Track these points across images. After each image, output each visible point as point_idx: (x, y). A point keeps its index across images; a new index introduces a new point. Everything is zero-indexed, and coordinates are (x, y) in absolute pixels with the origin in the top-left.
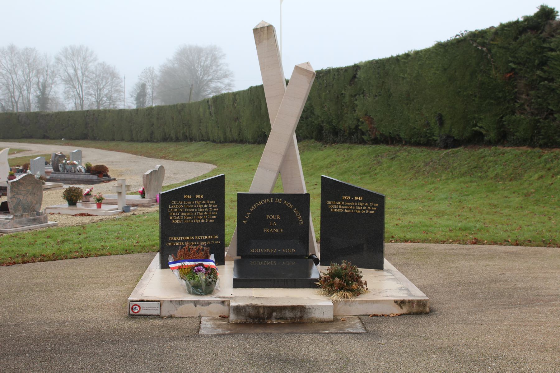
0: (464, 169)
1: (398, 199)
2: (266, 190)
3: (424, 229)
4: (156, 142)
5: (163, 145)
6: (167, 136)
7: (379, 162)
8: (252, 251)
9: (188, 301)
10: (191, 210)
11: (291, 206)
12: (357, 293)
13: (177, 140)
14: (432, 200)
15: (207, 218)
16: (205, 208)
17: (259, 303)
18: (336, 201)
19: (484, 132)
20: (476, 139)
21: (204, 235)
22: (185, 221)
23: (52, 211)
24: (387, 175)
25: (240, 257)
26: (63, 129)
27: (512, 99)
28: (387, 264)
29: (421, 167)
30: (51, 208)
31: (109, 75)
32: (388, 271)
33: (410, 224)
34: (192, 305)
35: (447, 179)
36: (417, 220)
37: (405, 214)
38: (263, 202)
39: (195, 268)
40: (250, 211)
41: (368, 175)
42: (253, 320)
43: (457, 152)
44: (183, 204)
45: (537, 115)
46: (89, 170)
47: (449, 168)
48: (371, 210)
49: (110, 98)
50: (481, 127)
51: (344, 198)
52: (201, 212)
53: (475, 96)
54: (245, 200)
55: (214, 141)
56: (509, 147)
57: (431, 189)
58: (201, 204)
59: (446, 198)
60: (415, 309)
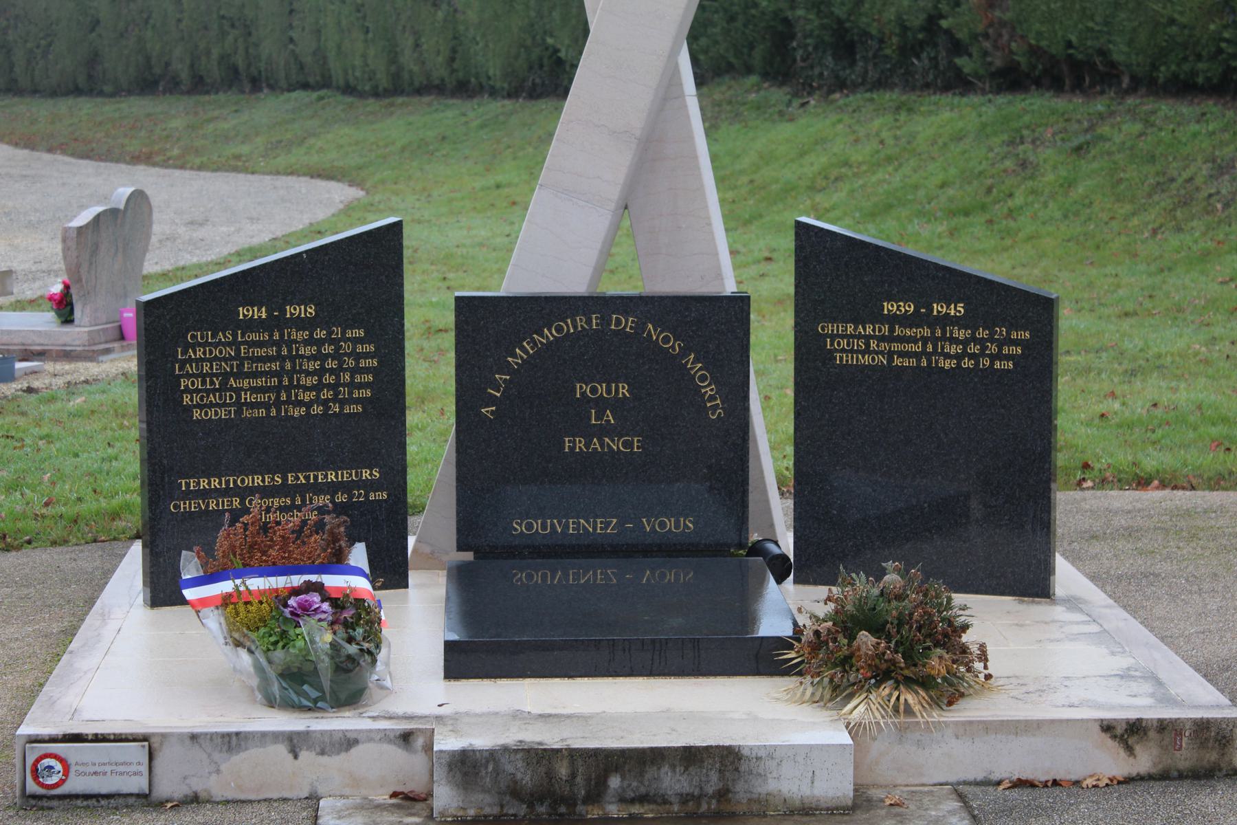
1: (1106, 311)
2: (572, 280)
3: (1214, 431)
4: (112, 95)
5: (138, 106)
6: (157, 70)
7: (1024, 164)
8: (519, 527)
9: (264, 735)
11: (675, 346)
12: (947, 692)
13: (199, 85)
17: (551, 738)
18: (856, 323)
21: (324, 467)
22: (247, 413)
24: (1058, 214)
25: (468, 556)
28: (1067, 575)
29: (1199, 181)
32: (1073, 603)
33: (1158, 412)
34: (282, 750)
36: (1185, 396)
37: (1133, 373)
38: (559, 330)
39: (292, 602)
40: (506, 368)
41: (979, 219)
42: (531, 806)
44: (234, 343)
48: (999, 356)
51: (889, 307)
52: (308, 373)
54: (486, 324)
55: (349, 90)
58: (307, 342)
60: (1185, 757)
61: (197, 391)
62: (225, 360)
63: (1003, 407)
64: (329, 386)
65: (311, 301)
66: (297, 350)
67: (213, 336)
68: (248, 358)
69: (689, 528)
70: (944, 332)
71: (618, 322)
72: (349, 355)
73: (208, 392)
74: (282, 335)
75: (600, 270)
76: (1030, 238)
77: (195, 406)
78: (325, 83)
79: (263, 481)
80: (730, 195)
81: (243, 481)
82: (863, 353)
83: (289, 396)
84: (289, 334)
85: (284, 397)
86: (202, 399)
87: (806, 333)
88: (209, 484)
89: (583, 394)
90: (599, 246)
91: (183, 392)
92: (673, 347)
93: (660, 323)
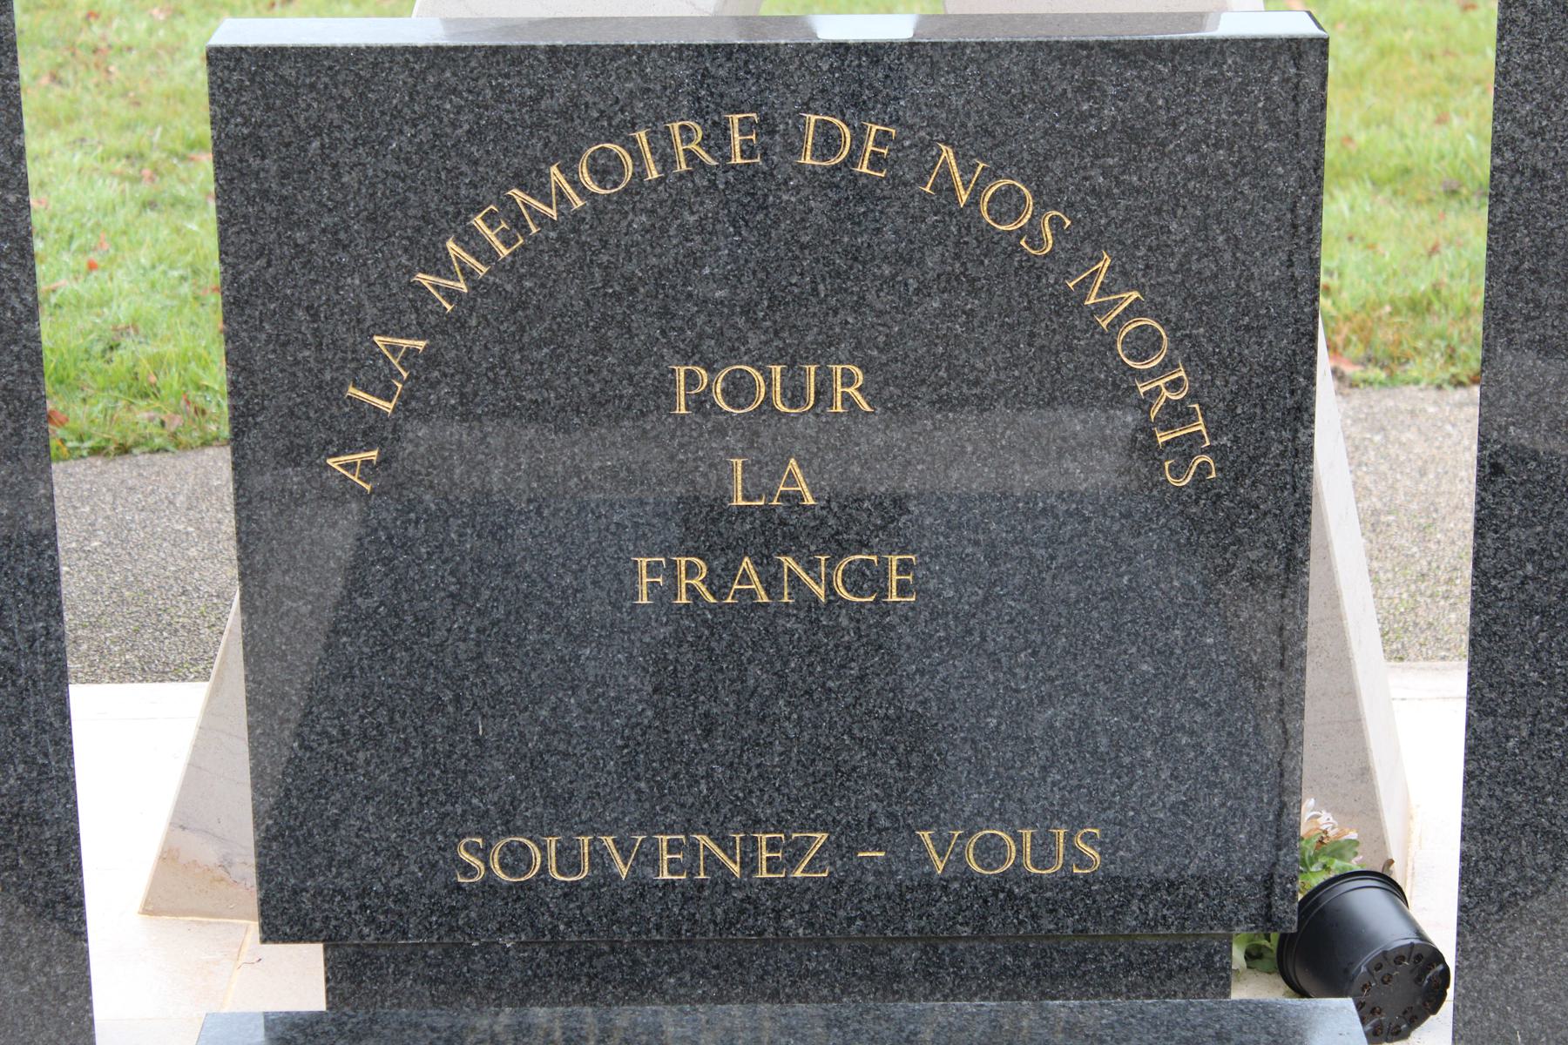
8: (479, 862)
40: (409, 310)
69: (1083, 861)
71: (828, 142)
80: (1498, 161)
87: (1538, 174)
89: (701, 403)
92: (1033, 233)
93: (985, 142)
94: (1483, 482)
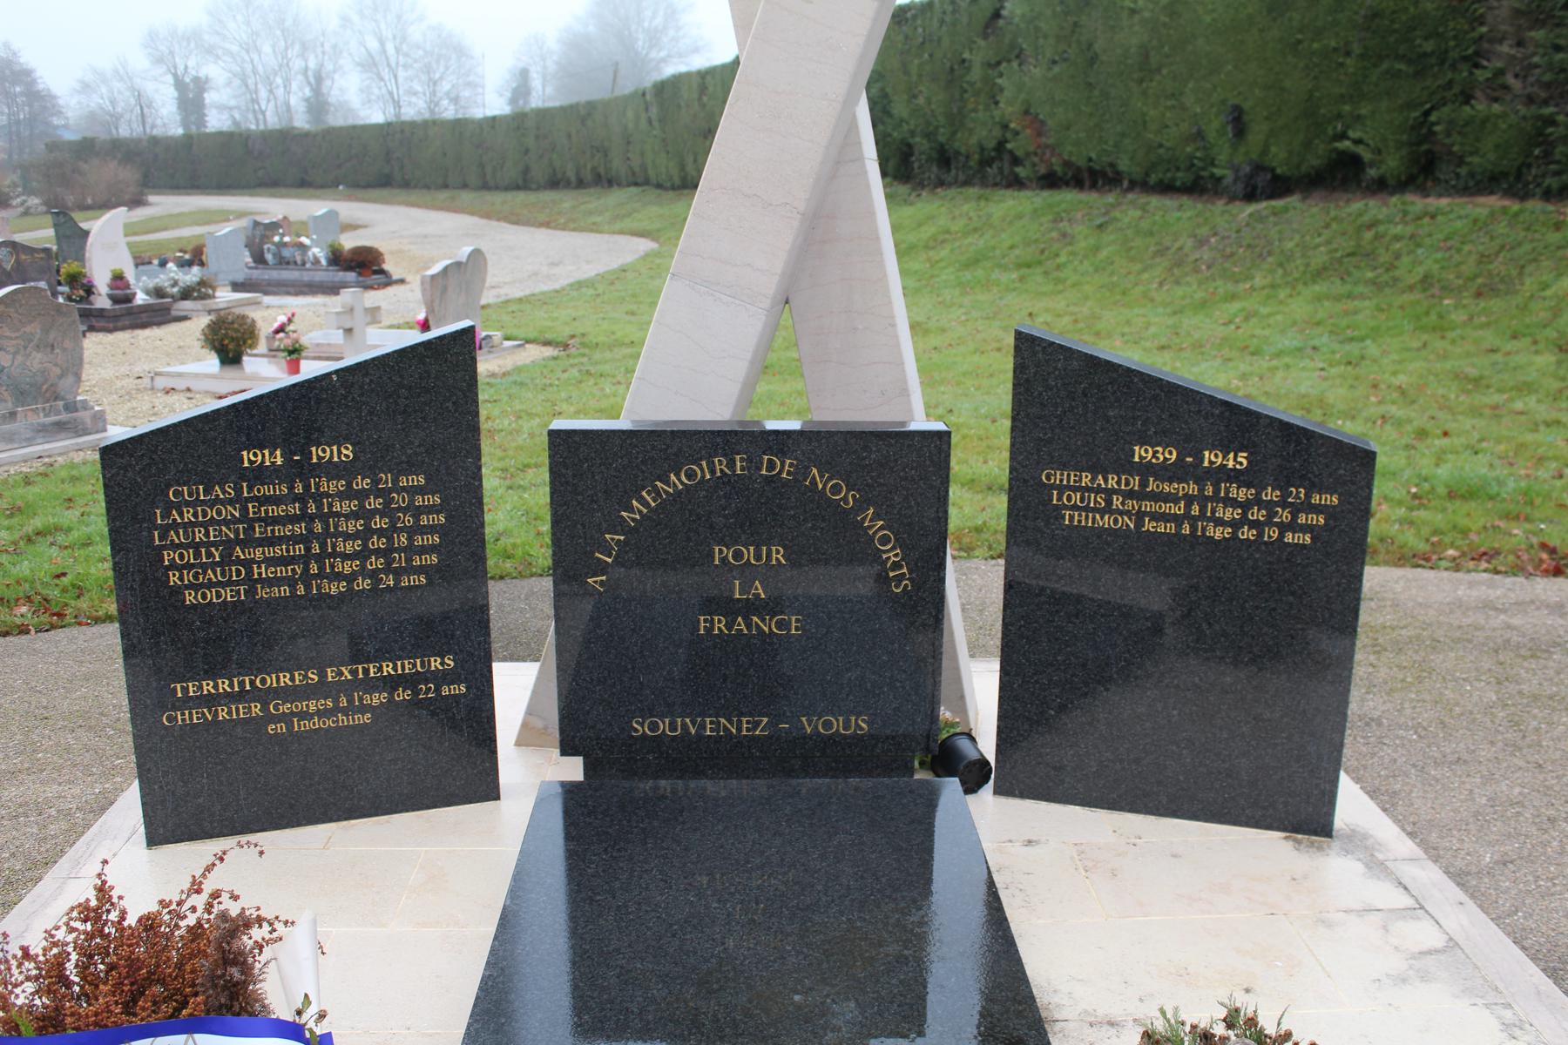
0: (1319, 258)
1: (1148, 344)
5: (548, 196)
7: (1064, 235)
8: (640, 728)
10: (287, 530)
13: (581, 184)
14: (1253, 354)
15: (388, 569)
16: (368, 515)
18: (1095, 470)
19: (1367, 155)
20: (1340, 174)
22: (262, 593)
23: (170, 383)
24: (1091, 269)
26: (339, 166)
27: (1465, 59)
28: (1352, 804)
29: (1186, 250)
30: (168, 375)
31: (453, 50)
35: (1273, 286)
40: (619, 526)
41: (1039, 270)
43: (1286, 210)
44: (238, 500)
45: (1546, 103)
46: (339, 259)
47: (1270, 253)
48: (1293, 526)
49: (455, 100)
50: (1358, 142)
51: (1141, 453)
52: (347, 537)
53: (1348, 54)
55: (659, 186)
56: (1440, 196)
57: (1236, 316)
58: (342, 496)
59: (1300, 350)
61: (189, 566)
62: (226, 522)
63: (1293, 593)
64: (378, 552)
65: (347, 439)
66: (330, 506)
67: (206, 492)
68: (260, 519)
69: (862, 729)
70: (1217, 491)
71: (771, 465)
72: (405, 510)
73: (205, 567)
74: (307, 487)
75: (747, 396)
76: (1074, 285)
77: (187, 587)
78: (647, 182)
79: (292, 679)
81: (263, 681)
82: (1102, 512)
83: (322, 568)
84: (318, 486)
85: (314, 568)
86: (196, 576)
87: (1025, 481)
88: (216, 687)
89: (724, 560)
90: (749, 356)
91: (168, 568)
92: (845, 499)
94: (1006, 592)
